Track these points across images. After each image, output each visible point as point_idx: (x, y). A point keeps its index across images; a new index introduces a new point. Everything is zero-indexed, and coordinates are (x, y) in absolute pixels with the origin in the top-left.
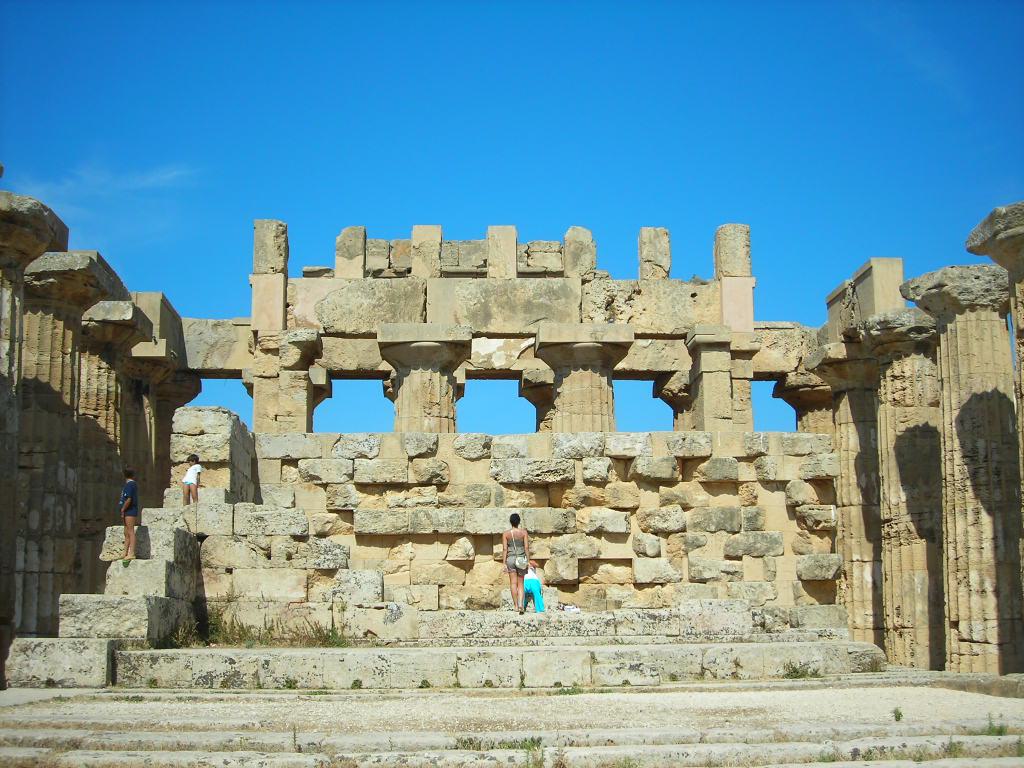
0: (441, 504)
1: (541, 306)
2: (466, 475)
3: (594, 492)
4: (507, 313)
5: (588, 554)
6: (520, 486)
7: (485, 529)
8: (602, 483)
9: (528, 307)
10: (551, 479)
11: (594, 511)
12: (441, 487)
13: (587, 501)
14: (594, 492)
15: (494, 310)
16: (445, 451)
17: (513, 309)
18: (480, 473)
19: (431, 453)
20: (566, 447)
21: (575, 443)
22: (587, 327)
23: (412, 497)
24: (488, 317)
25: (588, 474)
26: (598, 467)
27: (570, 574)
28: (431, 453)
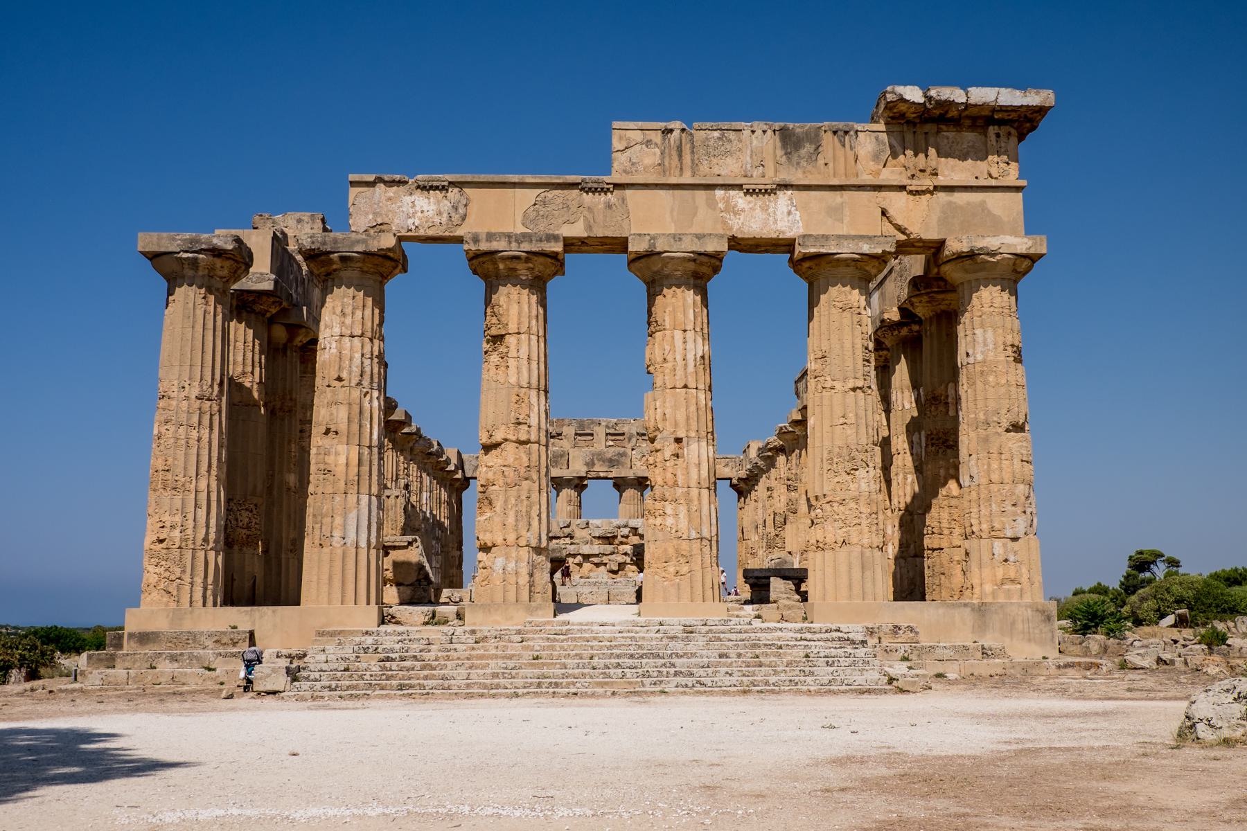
0: (572, 544)
1: (614, 460)
2: (579, 534)
3: (624, 540)
4: (601, 463)
5: (622, 561)
6: (599, 538)
7: (586, 552)
8: (627, 537)
9: (610, 460)
10: (609, 535)
11: (624, 546)
12: (572, 538)
13: (622, 543)
14: (624, 540)
15: (596, 462)
16: (573, 527)
17: (603, 461)
18: (585, 534)
19: (568, 526)
20: (615, 524)
21: (618, 522)
22: (632, 472)
23: (562, 541)
24: (593, 464)
25: (622, 534)
26: (626, 531)
27: (616, 568)
28: (568, 526)
